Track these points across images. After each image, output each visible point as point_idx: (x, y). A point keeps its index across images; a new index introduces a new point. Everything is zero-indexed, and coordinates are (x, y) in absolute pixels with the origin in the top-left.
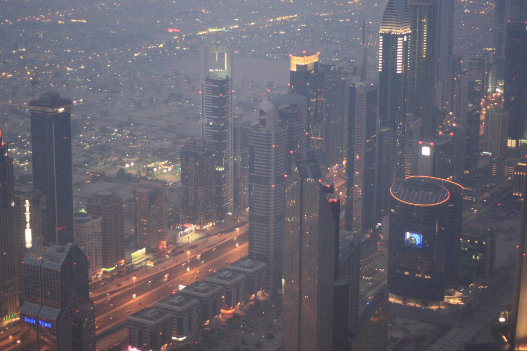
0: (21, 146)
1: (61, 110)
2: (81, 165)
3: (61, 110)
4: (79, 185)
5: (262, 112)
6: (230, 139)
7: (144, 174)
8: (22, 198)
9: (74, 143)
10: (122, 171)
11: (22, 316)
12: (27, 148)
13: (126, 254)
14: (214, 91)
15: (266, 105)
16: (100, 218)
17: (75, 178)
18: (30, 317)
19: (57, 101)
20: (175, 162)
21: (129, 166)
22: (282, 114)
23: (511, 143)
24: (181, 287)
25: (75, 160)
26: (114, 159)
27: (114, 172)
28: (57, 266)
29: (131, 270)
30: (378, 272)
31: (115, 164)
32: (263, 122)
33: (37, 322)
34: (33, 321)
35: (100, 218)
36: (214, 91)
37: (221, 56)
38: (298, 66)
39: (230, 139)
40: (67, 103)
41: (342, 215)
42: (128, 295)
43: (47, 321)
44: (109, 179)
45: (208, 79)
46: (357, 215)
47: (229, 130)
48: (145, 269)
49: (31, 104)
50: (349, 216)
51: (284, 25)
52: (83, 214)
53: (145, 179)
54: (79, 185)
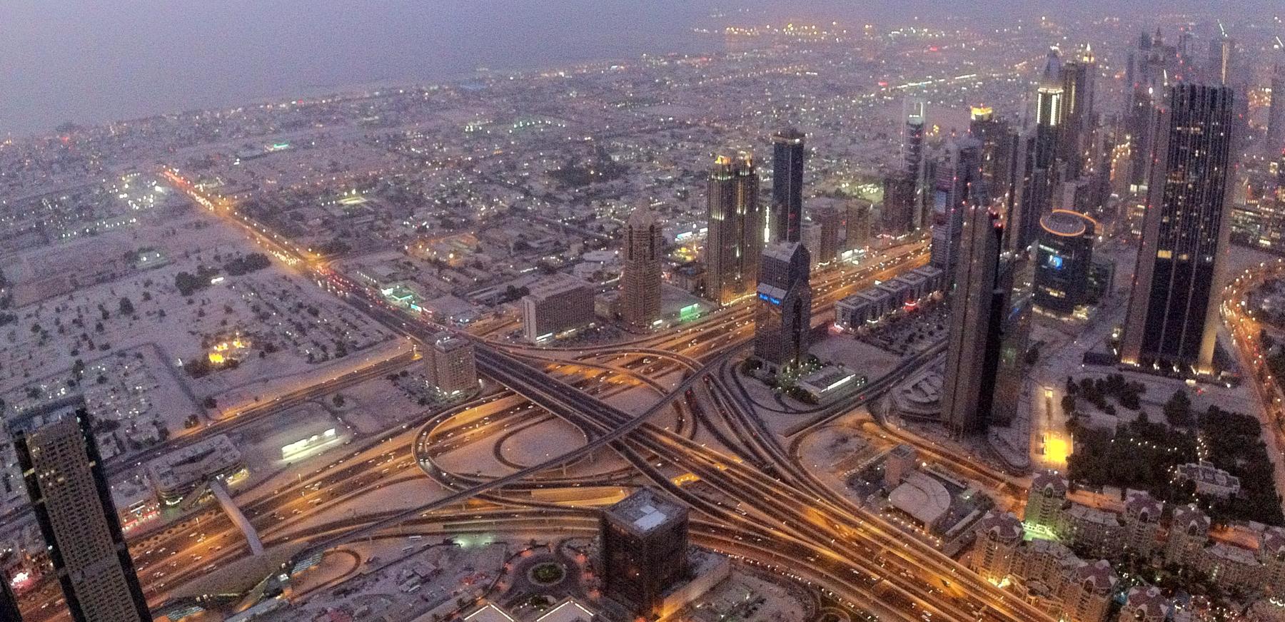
0: (766, 167)
1: (797, 141)
2: (808, 184)
3: (797, 141)
4: (805, 198)
5: (947, 152)
6: (921, 171)
7: (855, 194)
8: (764, 205)
9: (805, 166)
11: (759, 293)
12: (769, 168)
13: (838, 252)
14: (912, 133)
15: (951, 146)
16: (821, 225)
17: (804, 193)
18: (764, 295)
19: (794, 134)
20: (879, 186)
22: (963, 155)
25: (805, 180)
26: (834, 181)
27: (833, 190)
28: (787, 259)
29: (841, 265)
31: (834, 185)
32: (948, 159)
34: (766, 298)
35: (821, 225)
36: (912, 133)
39: (921, 171)
40: (802, 136)
41: (1003, 237)
42: (836, 285)
43: (776, 299)
44: (829, 196)
45: (908, 123)
46: (1014, 237)
47: (922, 163)
48: (851, 266)
49: (776, 135)
50: (1008, 237)
52: (808, 221)
53: (856, 197)
54: (805, 198)
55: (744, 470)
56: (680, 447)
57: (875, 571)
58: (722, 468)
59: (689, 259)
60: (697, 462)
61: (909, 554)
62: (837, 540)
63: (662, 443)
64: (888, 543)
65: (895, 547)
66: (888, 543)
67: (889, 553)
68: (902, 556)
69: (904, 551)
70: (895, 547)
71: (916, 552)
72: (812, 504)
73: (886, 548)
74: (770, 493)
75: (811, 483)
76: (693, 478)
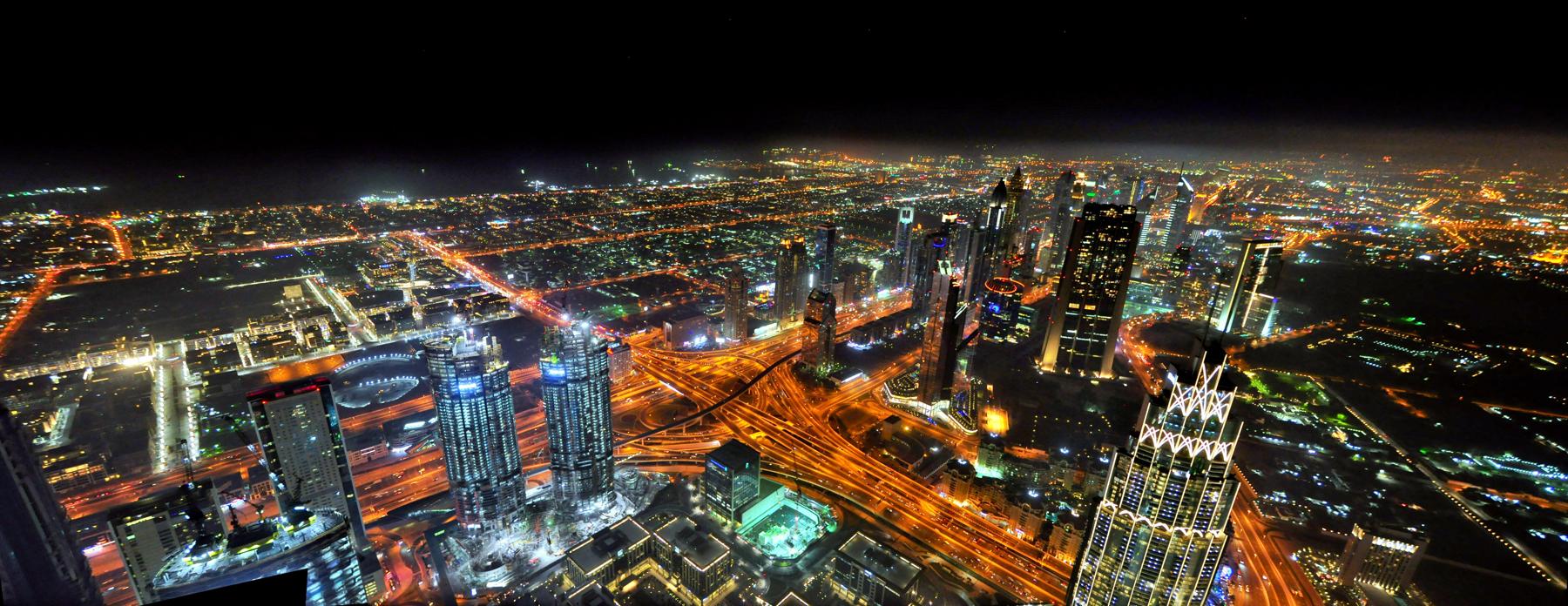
10: (856, 261)
21: (861, 260)
23: (1053, 266)
37: (909, 212)
46: (967, 294)
51: (942, 200)
55: (794, 430)
56: (756, 415)
57: (878, 495)
58: (780, 428)
59: (764, 301)
61: (899, 484)
63: (744, 412)
64: (885, 477)
65: (890, 480)
66: (885, 477)
67: (886, 485)
68: (894, 485)
70: (890, 480)
71: (903, 483)
72: (836, 452)
73: (883, 481)
74: (810, 445)
76: (763, 434)
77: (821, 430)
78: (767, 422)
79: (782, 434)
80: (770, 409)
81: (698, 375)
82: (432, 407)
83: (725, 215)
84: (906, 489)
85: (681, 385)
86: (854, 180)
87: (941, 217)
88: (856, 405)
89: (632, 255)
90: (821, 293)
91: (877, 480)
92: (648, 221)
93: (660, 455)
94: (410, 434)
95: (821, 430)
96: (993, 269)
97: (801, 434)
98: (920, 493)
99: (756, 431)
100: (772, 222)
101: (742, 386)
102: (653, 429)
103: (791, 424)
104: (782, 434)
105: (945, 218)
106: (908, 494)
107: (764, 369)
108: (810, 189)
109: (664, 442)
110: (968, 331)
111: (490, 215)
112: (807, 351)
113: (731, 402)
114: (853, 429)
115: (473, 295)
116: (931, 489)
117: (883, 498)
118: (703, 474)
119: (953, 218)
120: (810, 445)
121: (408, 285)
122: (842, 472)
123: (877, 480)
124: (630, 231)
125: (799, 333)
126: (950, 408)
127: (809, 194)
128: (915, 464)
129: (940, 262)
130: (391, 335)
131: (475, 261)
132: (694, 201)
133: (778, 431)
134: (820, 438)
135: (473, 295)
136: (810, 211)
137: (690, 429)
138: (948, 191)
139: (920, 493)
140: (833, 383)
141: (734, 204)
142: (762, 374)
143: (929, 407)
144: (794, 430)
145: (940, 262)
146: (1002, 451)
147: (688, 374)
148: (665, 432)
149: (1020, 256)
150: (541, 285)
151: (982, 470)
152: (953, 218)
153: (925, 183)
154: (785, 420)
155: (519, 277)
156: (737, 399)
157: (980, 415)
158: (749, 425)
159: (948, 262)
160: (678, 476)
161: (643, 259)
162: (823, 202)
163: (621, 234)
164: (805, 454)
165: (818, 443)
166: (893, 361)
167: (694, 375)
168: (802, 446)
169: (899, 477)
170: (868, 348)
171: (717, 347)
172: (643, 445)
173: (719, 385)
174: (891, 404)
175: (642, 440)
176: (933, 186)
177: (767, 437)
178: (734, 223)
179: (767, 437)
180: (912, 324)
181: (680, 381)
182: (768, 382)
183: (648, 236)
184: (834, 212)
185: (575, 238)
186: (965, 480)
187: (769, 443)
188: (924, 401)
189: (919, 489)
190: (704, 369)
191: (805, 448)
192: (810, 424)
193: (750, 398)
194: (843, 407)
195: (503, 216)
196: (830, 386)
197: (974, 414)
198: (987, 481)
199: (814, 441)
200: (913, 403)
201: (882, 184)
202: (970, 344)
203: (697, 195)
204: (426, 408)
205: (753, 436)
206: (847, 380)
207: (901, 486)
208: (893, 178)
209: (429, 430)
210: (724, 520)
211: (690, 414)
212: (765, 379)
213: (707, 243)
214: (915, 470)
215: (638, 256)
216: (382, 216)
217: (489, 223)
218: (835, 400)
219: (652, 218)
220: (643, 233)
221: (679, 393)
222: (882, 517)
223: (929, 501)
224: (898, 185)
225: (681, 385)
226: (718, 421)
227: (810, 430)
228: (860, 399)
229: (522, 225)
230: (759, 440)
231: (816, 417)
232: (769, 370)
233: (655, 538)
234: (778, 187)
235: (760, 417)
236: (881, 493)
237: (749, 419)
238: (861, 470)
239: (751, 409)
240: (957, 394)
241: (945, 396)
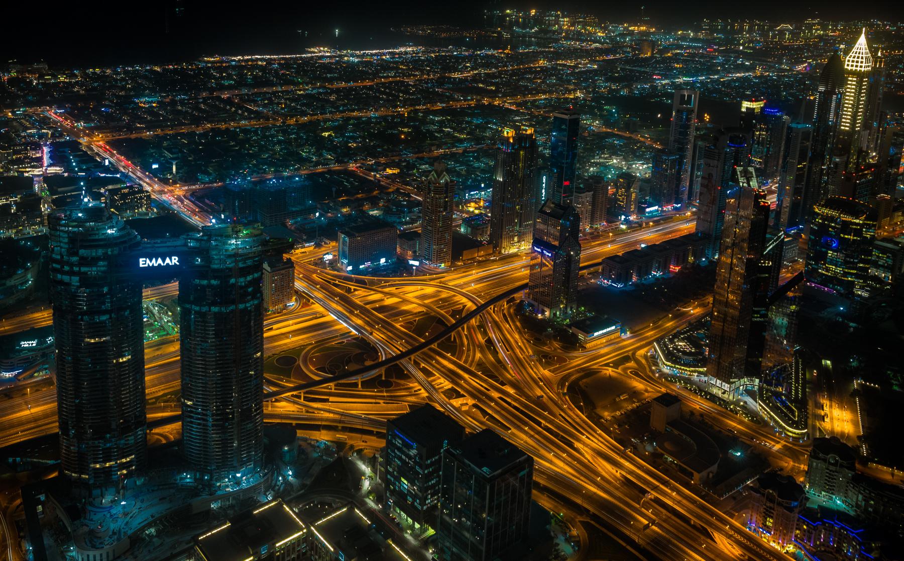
11: (533, 246)
24: (643, 246)
30: (797, 260)
33: (542, 250)
38: (747, 108)
55: (516, 400)
58: (495, 395)
60: (474, 387)
62: (603, 478)
63: (444, 367)
64: (655, 488)
66: (655, 488)
67: (657, 501)
69: (671, 498)
72: (579, 440)
73: (654, 494)
74: (539, 424)
75: (578, 420)
76: (471, 402)
77: (556, 404)
78: (475, 382)
79: (497, 403)
80: (480, 365)
81: (382, 309)
82: (50, 323)
83: (430, 96)
84: (689, 511)
85: (359, 322)
86: (607, 52)
87: (740, 105)
88: (610, 371)
89: (304, 145)
90: (558, 205)
91: (644, 492)
92: (328, 101)
93: (327, 415)
94: (22, 355)
95: (556, 404)
96: (827, 183)
97: (526, 406)
98: (714, 520)
99: (459, 395)
100: (491, 106)
101: (443, 329)
102: (317, 378)
103: (511, 391)
104: (497, 403)
105: (746, 105)
106: (694, 520)
107: (474, 307)
108: (542, 63)
109: (331, 399)
110: (786, 275)
111: (139, 91)
112: (536, 286)
113: (425, 349)
114: (605, 408)
115: (110, 187)
116: (732, 516)
117: (653, 523)
118: (382, 450)
119: (756, 106)
120: (539, 424)
121: (37, 172)
122: (589, 471)
123: (644, 492)
124: (304, 114)
125: (525, 261)
126: (761, 389)
127: (544, 70)
128: (704, 473)
129: (739, 169)
130: (14, 231)
131: (115, 145)
132: (388, 77)
133: (491, 399)
134: (551, 413)
135: (110, 187)
136: (544, 93)
137: (367, 384)
138: (752, 68)
139: (714, 520)
140: (575, 336)
141: (441, 82)
142: (472, 314)
143: (726, 386)
144: (516, 400)
145: (739, 169)
146: (852, 468)
147: (367, 306)
148: (332, 384)
149: (869, 166)
150: (187, 178)
151: (819, 498)
152: (756, 106)
153: (715, 58)
154: (503, 384)
155: (165, 168)
156: (434, 346)
157: (810, 406)
158: (450, 386)
159: (751, 169)
160: (340, 445)
161: (318, 150)
162: (563, 81)
163: (292, 117)
164: (531, 436)
165: (551, 422)
166: (669, 311)
167: (375, 309)
168: (526, 424)
169: (679, 492)
170: (628, 288)
171: (408, 270)
172: (302, 400)
173: (409, 324)
174: (663, 375)
175: (302, 393)
176: (727, 61)
177: (475, 406)
178: (440, 106)
179: (475, 406)
180: (697, 256)
181: (357, 316)
182: (479, 327)
183: (326, 121)
184: (578, 94)
185: (234, 120)
186: (791, 510)
187: (480, 415)
188: (718, 376)
189: (712, 514)
190: (389, 301)
191: (531, 428)
192: (539, 392)
193: (453, 347)
194: (589, 373)
195: (153, 91)
196: (571, 343)
197: (802, 404)
198: (828, 514)
199: (545, 418)
200: (697, 375)
201: (652, 57)
202: (790, 294)
203: (392, 69)
204: (44, 324)
205: (457, 402)
206: (596, 334)
207: (683, 506)
208: (667, 49)
209: (42, 353)
210: (410, 520)
211: (368, 363)
212: (473, 322)
213: (403, 133)
214: (706, 482)
215: (312, 145)
216: (22, 90)
217: (136, 101)
218: (578, 360)
219: (333, 98)
220: (320, 117)
221: (354, 332)
222: (649, 548)
223: (729, 537)
224: (676, 58)
225: (359, 322)
226: (410, 378)
227: (538, 401)
228: (616, 364)
229: (173, 103)
230: (464, 408)
231: (548, 382)
232: (480, 309)
233: (313, 534)
234: (499, 60)
235: (466, 376)
236: (649, 513)
237: (451, 375)
238: (618, 473)
239: (454, 363)
240: (771, 369)
241: (752, 370)
